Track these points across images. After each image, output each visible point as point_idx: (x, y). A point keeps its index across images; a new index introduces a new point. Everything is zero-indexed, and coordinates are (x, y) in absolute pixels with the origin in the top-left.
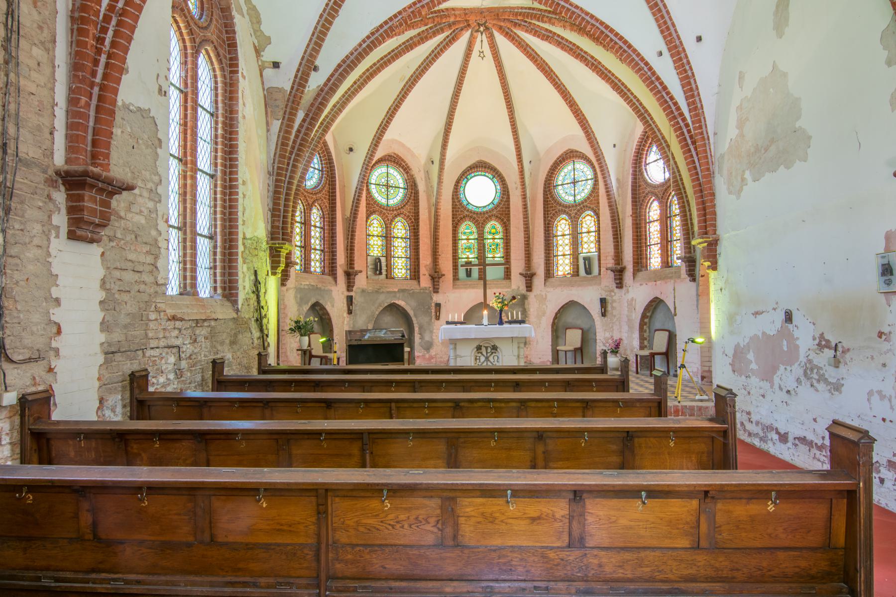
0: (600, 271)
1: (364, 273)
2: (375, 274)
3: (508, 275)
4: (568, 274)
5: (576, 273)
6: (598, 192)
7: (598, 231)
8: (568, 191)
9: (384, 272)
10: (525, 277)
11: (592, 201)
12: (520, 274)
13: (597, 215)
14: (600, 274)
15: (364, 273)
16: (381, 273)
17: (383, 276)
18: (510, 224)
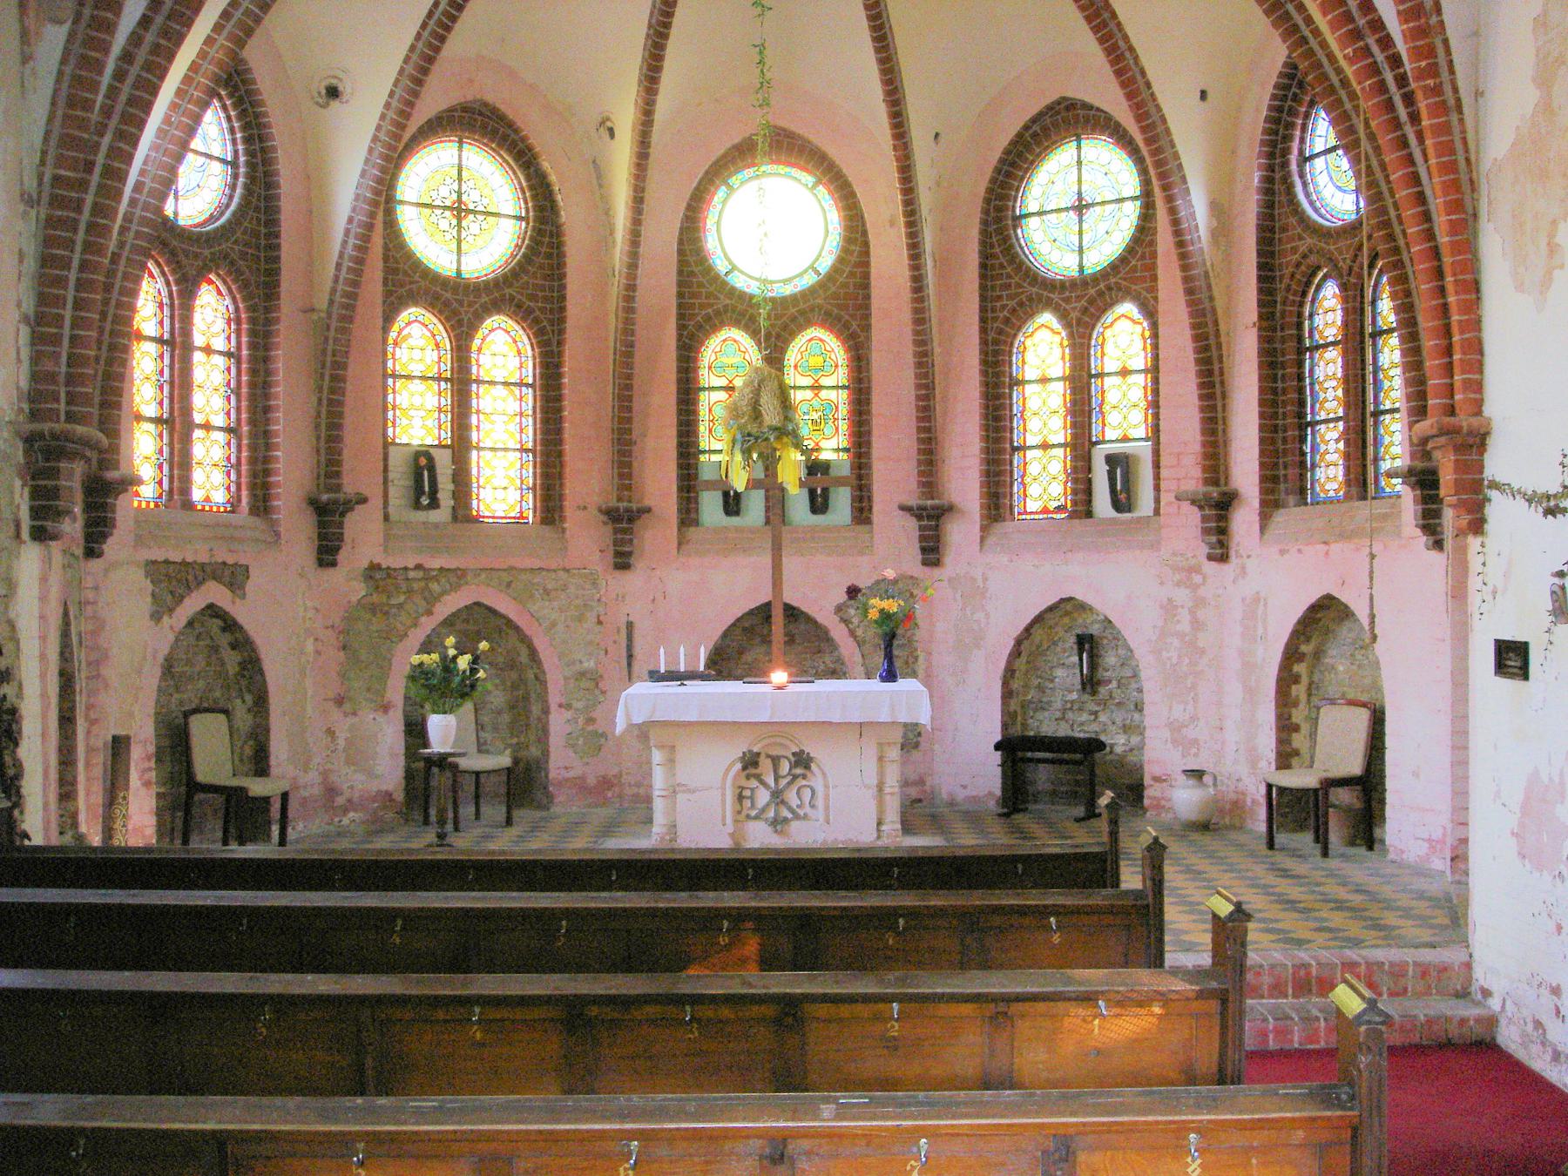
0: (1157, 500)
1: (376, 502)
2: (417, 505)
3: (862, 512)
4: (1059, 509)
5: (1082, 504)
6: (1152, 243)
7: (1154, 370)
8: (1058, 234)
9: (445, 498)
10: (919, 518)
11: (1134, 270)
12: (903, 508)
13: (1150, 312)
14: (1157, 511)
15: (373, 509)
16: (434, 504)
17: (442, 515)
18: (868, 338)
